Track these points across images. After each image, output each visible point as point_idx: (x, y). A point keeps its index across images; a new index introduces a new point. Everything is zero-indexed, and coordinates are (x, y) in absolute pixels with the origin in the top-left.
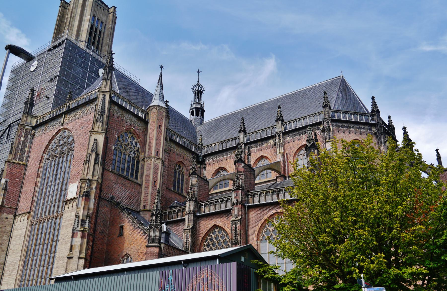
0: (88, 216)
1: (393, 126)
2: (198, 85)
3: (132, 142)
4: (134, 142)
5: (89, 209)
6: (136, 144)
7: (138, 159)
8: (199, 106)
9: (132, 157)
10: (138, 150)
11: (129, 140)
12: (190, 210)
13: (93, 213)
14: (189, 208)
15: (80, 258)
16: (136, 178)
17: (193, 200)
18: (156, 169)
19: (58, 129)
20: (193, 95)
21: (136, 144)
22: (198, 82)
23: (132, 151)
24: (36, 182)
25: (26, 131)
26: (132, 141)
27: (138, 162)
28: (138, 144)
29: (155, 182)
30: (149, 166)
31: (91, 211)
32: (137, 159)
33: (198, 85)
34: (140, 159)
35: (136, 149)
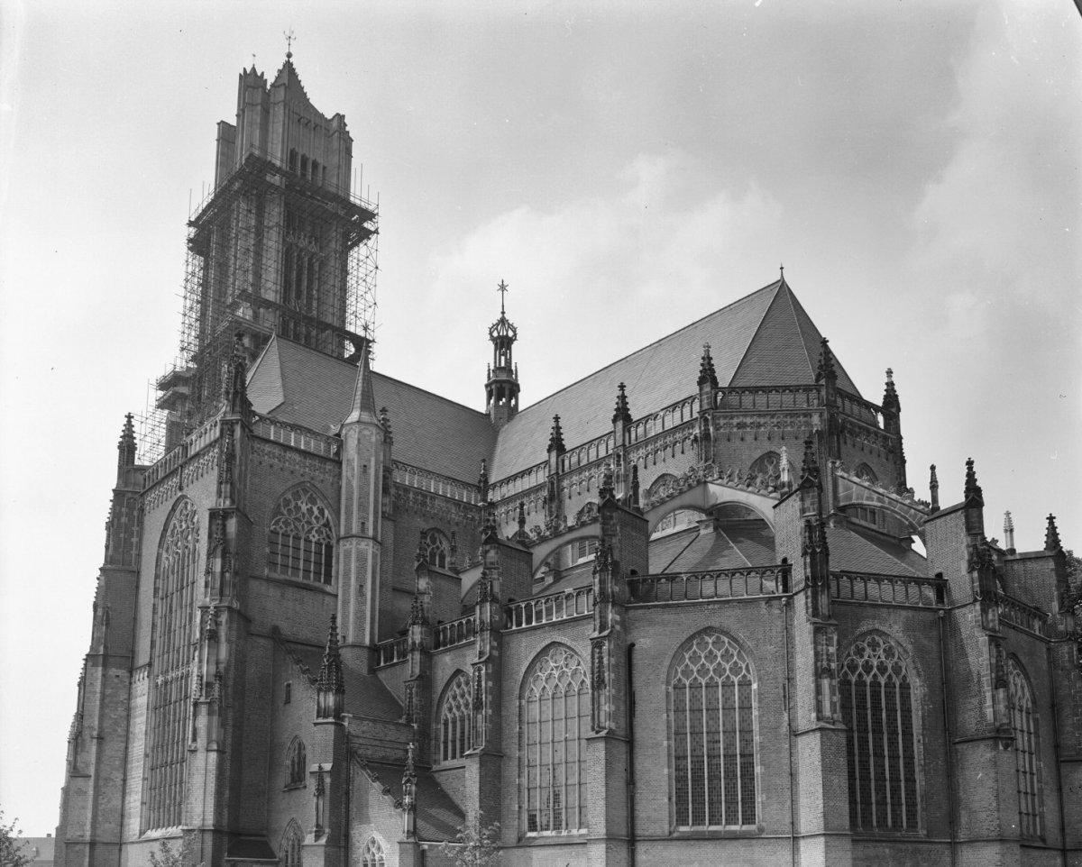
0: (218, 676)
1: (897, 396)
2: (503, 321)
3: (310, 511)
4: (315, 509)
5: (218, 663)
6: (321, 511)
7: (329, 542)
8: (503, 377)
9: (314, 540)
10: (327, 525)
11: (304, 508)
12: (414, 643)
13: (227, 670)
14: (412, 639)
15: (208, 751)
16: (328, 581)
17: (418, 623)
18: (362, 559)
19: (175, 498)
20: (492, 346)
21: (321, 511)
22: (503, 313)
23: (312, 528)
24: (154, 605)
25: (128, 503)
26: (311, 508)
27: (329, 547)
28: (326, 512)
29: (361, 586)
30: (348, 554)
31: (222, 666)
32: (324, 543)
33: (503, 321)
34: (334, 542)
35: (322, 522)
